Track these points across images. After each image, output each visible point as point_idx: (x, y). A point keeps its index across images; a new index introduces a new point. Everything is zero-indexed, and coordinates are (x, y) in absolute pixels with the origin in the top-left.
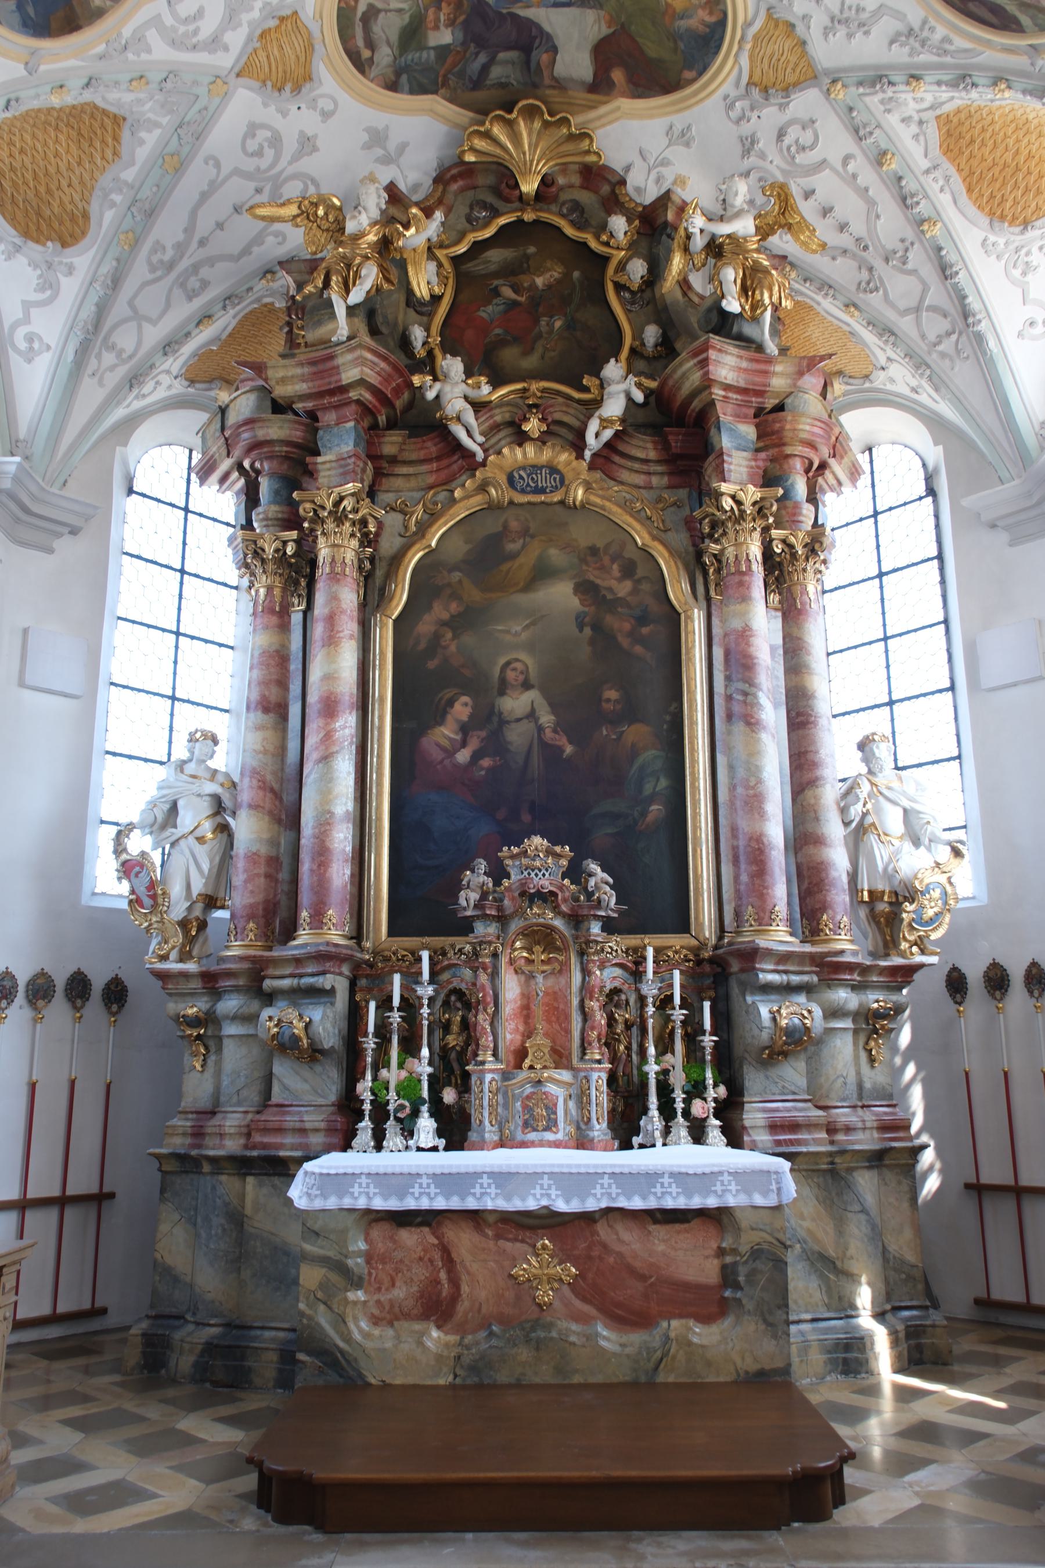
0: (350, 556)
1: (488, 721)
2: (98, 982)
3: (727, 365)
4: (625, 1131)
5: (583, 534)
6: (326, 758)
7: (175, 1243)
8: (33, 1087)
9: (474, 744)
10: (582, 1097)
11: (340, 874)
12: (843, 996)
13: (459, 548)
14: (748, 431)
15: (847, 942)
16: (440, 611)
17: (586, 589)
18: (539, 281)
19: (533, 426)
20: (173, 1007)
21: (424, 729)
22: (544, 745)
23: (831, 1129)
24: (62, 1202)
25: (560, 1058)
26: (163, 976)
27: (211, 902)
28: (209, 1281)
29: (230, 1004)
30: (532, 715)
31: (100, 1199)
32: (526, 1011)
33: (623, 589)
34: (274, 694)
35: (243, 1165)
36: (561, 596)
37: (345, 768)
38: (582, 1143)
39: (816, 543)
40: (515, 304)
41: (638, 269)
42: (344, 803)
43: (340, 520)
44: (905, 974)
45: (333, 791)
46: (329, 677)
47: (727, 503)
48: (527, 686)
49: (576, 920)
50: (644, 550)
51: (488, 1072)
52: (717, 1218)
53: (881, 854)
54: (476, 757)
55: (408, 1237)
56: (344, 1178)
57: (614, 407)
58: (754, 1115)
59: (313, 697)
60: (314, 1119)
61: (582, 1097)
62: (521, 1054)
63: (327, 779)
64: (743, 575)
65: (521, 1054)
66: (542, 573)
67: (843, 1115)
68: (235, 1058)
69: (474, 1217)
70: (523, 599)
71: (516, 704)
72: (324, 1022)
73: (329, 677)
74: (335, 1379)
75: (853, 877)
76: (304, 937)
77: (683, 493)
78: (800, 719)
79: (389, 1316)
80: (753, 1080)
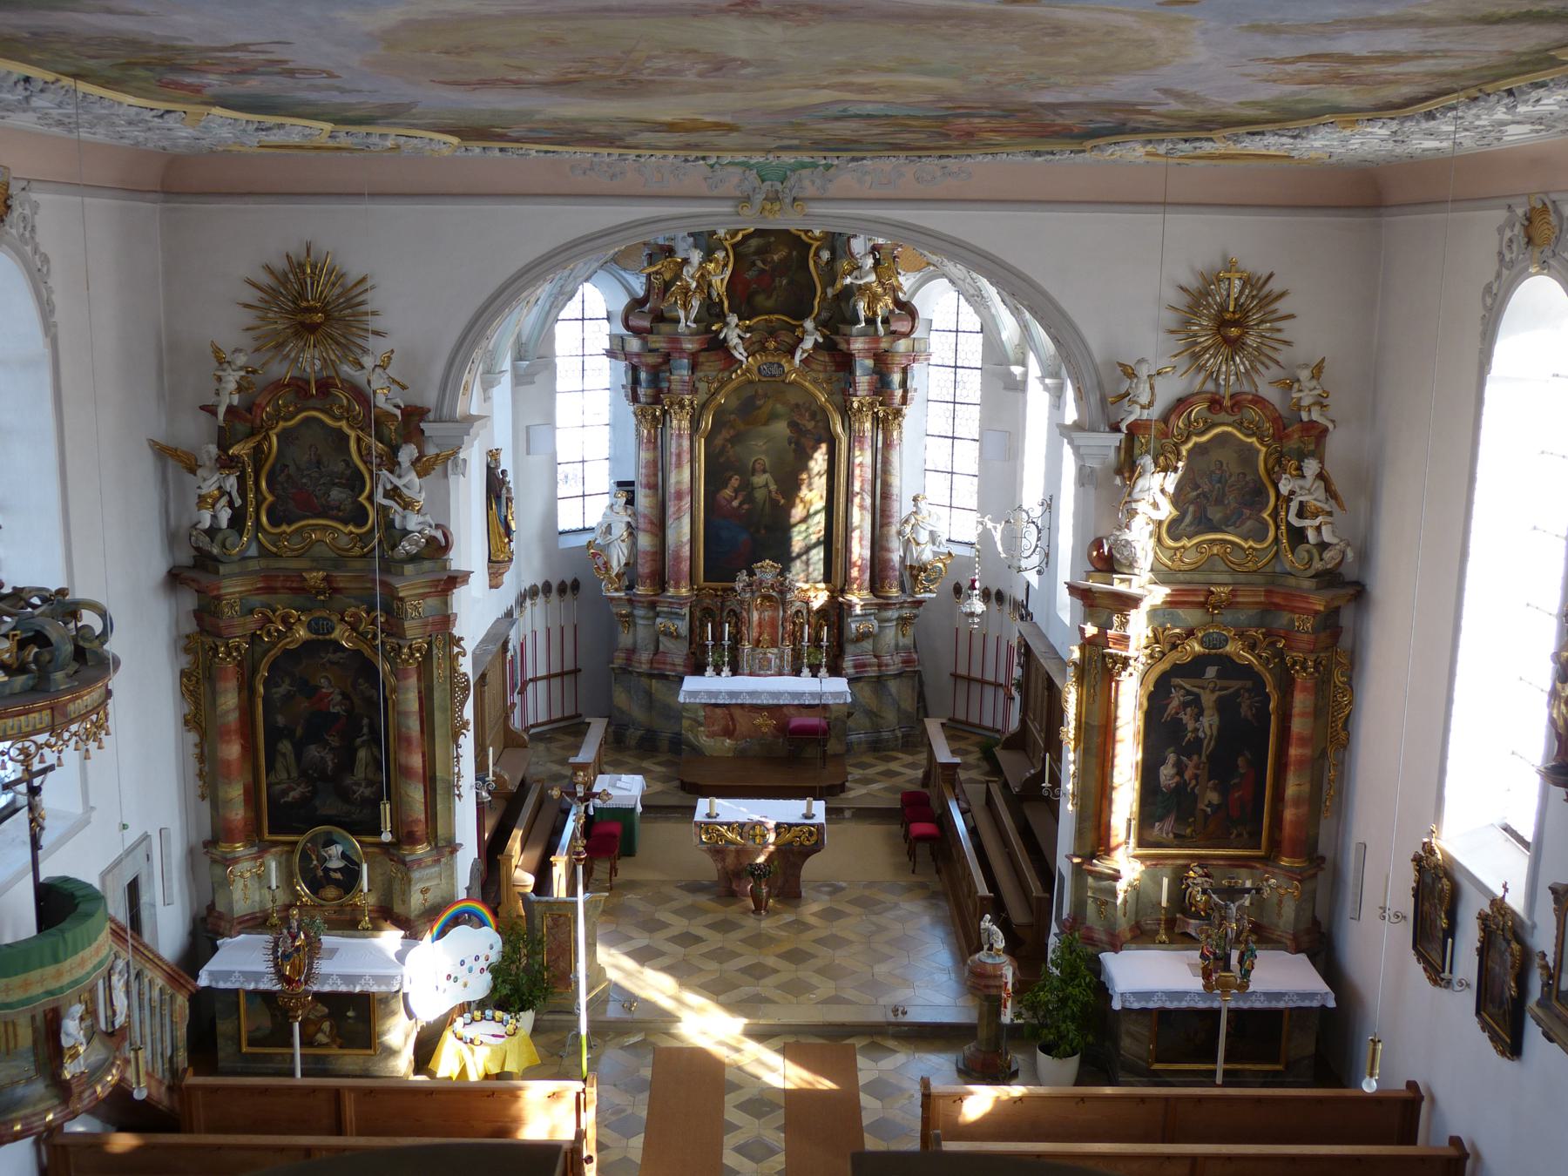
0: (685, 424)
1: (747, 488)
2: (569, 582)
3: (858, 345)
4: (797, 672)
5: (793, 397)
6: (679, 518)
7: (621, 698)
8: (548, 630)
9: (740, 498)
10: (781, 658)
11: (685, 566)
12: (892, 614)
13: (734, 403)
14: (870, 363)
15: (894, 592)
16: (726, 434)
17: (793, 425)
18: (776, 257)
19: (772, 345)
20: (615, 610)
21: (718, 490)
22: (772, 499)
23: (879, 666)
24: (562, 674)
25: (774, 644)
26: (612, 599)
27: (626, 564)
28: (638, 713)
29: (639, 612)
30: (766, 485)
31: (576, 671)
32: (760, 625)
33: (810, 425)
34: (652, 480)
35: (651, 676)
36: (781, 428)
37: (686, 520)
38: (780, 674)
39: (898, 413)
40: (762, 271)
41: (825, 255)
42: (686, 537)
43: (682, 407)
44: (919, 603)
45: (681, 531)
46: (678, 482)
47: (855, 405)
48: (764, 471)
49: (782, 593)
50: (823, 410)
51: (747, 647)
52: (825, 707)
53: (915, 550)
54: (741, 504)
55: (718, 711)
56: (695, 686)
57: (808, 344)
58: (848, 664)
59: (672, 489)
60: (679, 661)
61: (781, 658)
62: (758, 642)
63: (679, 527)
64: (861, 439)
65: (758, 642)
66: (773, 417)
67: (887, 659)
68: (643, 632)
69: (742, 706)
70: (764, 429)
71: (759, 479)
72: (683, 627)
73: (678, 482)
74: (696, 751)
75: (903, 559)
76: (671, 591)
77: (841, 374)
78: (886, 496)
79: (712, 735)
80: (850, 648)
